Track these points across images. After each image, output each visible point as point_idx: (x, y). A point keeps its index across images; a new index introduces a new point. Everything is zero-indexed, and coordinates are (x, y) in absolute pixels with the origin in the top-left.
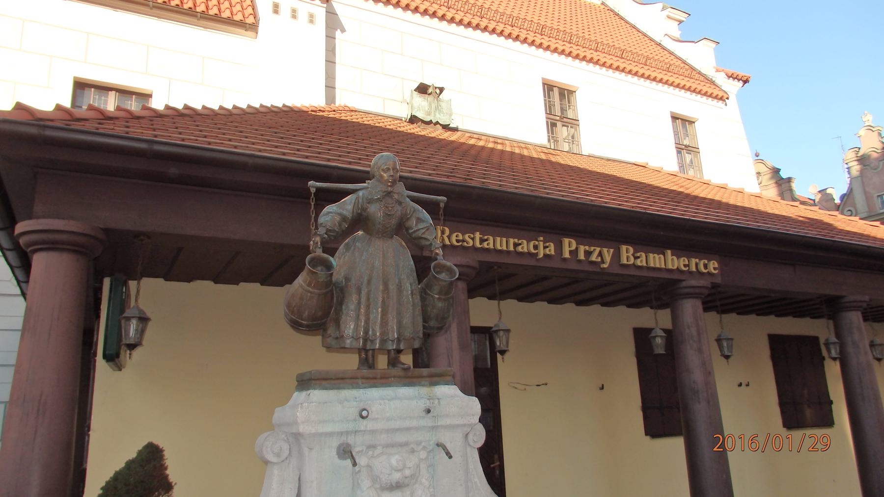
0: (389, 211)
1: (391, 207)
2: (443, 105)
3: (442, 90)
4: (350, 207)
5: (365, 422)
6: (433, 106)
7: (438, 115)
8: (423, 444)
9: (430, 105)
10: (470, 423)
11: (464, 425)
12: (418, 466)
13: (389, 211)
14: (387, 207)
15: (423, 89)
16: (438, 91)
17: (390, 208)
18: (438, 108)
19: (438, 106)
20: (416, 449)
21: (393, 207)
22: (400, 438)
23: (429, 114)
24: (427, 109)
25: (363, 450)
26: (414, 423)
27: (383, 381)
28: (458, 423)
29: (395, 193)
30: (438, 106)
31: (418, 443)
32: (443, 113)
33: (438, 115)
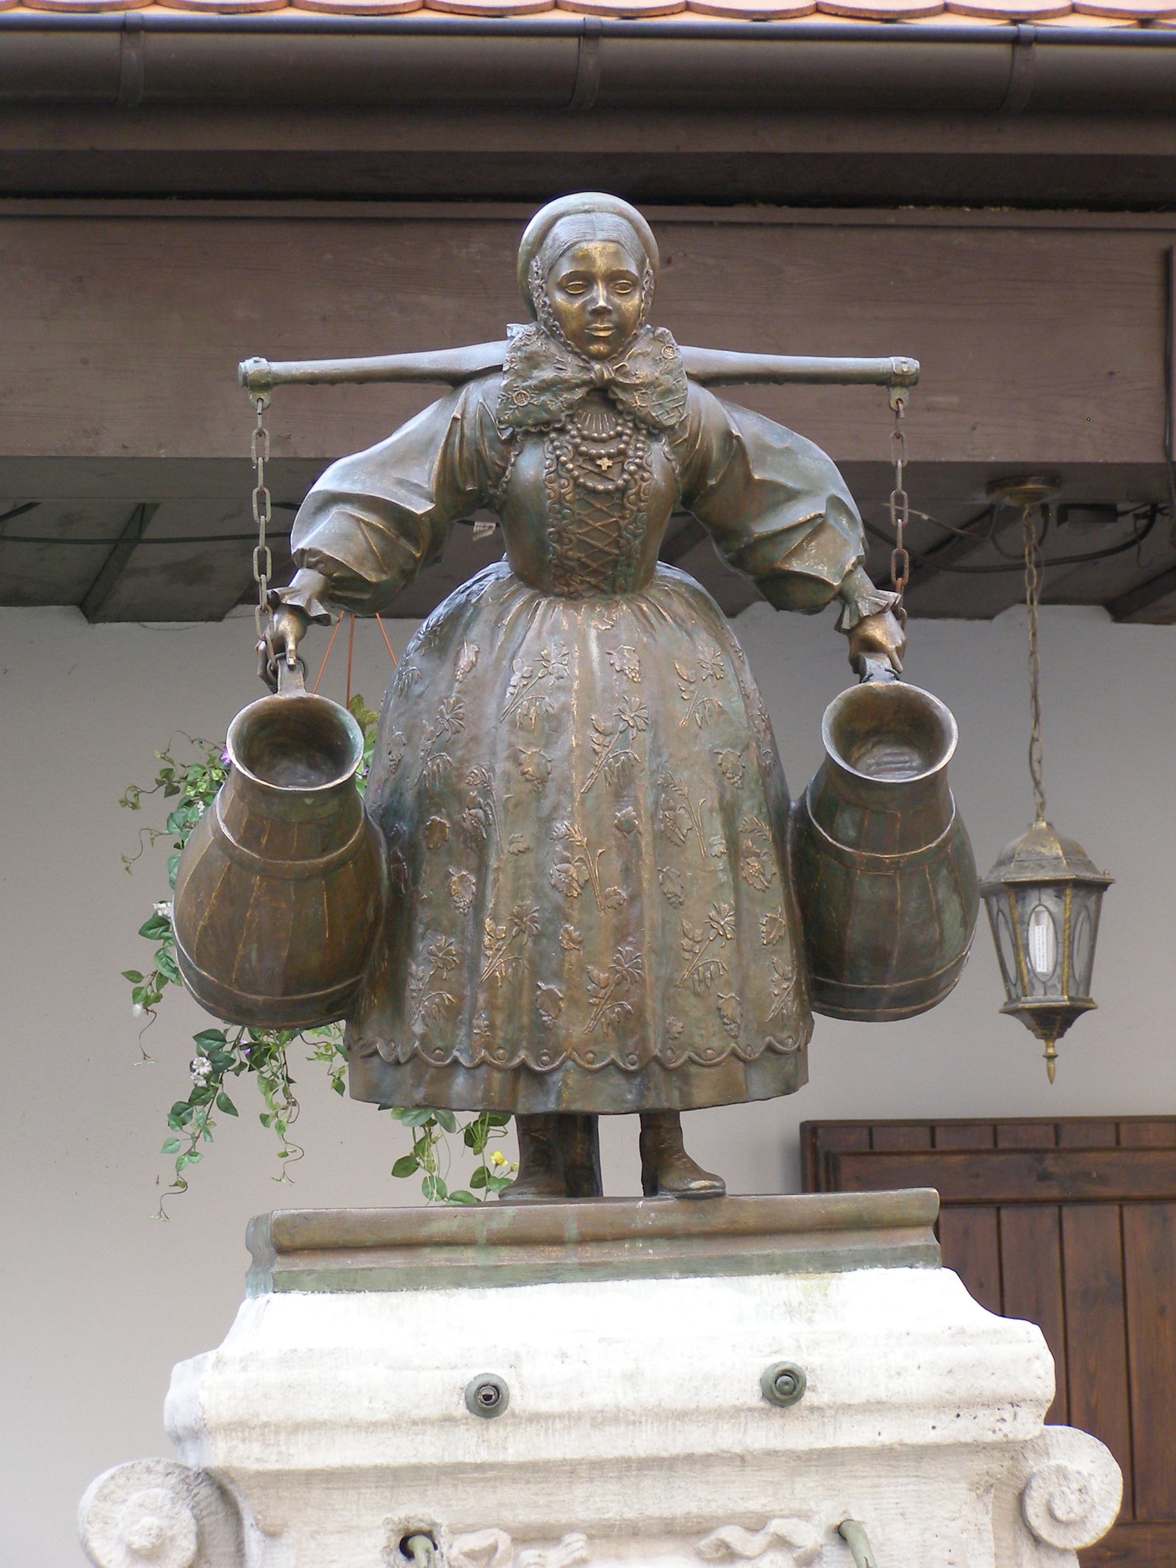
0: (602, 475)
1: (610, 456)
4: (425, 475)
5: (495, 1430)
8: (775, 1526)
10: (998, 1437)
11: (977, 1448)
13: (602, 475)
14: (592, 459)
17: (605, 463)
20: (738, 1546)
21: (622, 453)
25: (494, 1549)
26: (729, 1439)
27: (592, 1254)
28: (932, 1437)
29: (625, 388)
31: (755, 1524)
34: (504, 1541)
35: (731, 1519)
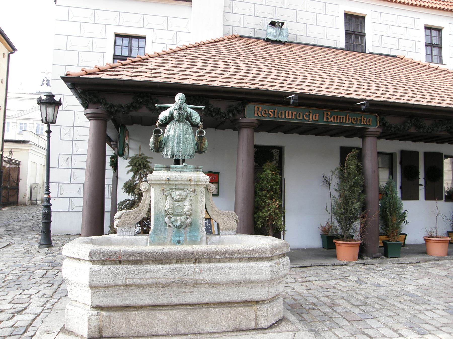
2: (284, 31)
3: (283, 23)
6: (278, 32)
7: (280, 37)
9: (276, 32)
12: (187, 196)
15: (273, 24)
16: (280, 24)
18: (281, 34)
19: (280, 32)
22: (181, 187)
23: (275, 37)
24: (274, 34)
30: (280, 32)
32: (283, 35)
33: (280, 37)
34: (169, 189)
35: (186, 188)
